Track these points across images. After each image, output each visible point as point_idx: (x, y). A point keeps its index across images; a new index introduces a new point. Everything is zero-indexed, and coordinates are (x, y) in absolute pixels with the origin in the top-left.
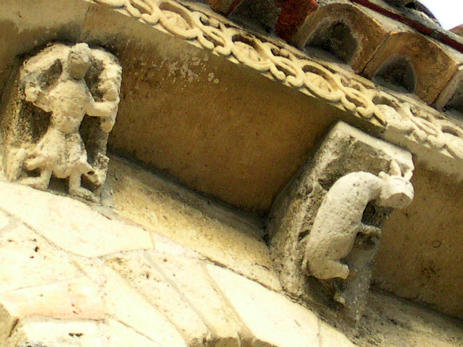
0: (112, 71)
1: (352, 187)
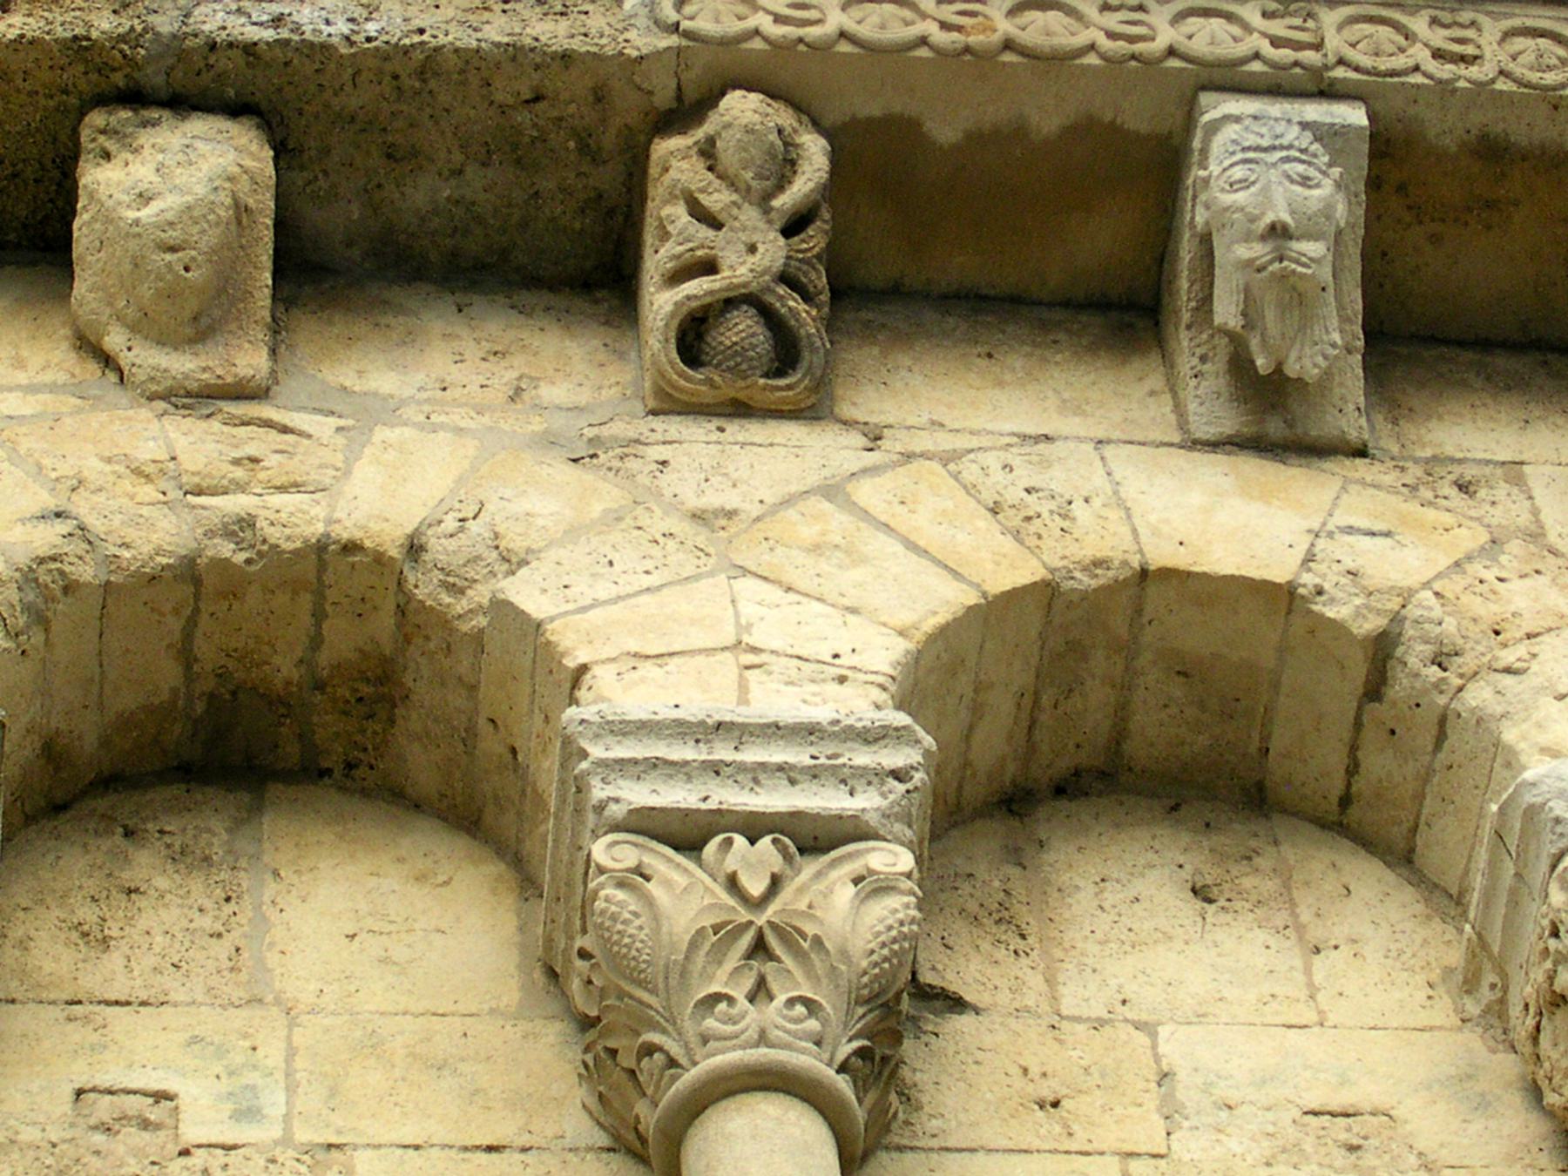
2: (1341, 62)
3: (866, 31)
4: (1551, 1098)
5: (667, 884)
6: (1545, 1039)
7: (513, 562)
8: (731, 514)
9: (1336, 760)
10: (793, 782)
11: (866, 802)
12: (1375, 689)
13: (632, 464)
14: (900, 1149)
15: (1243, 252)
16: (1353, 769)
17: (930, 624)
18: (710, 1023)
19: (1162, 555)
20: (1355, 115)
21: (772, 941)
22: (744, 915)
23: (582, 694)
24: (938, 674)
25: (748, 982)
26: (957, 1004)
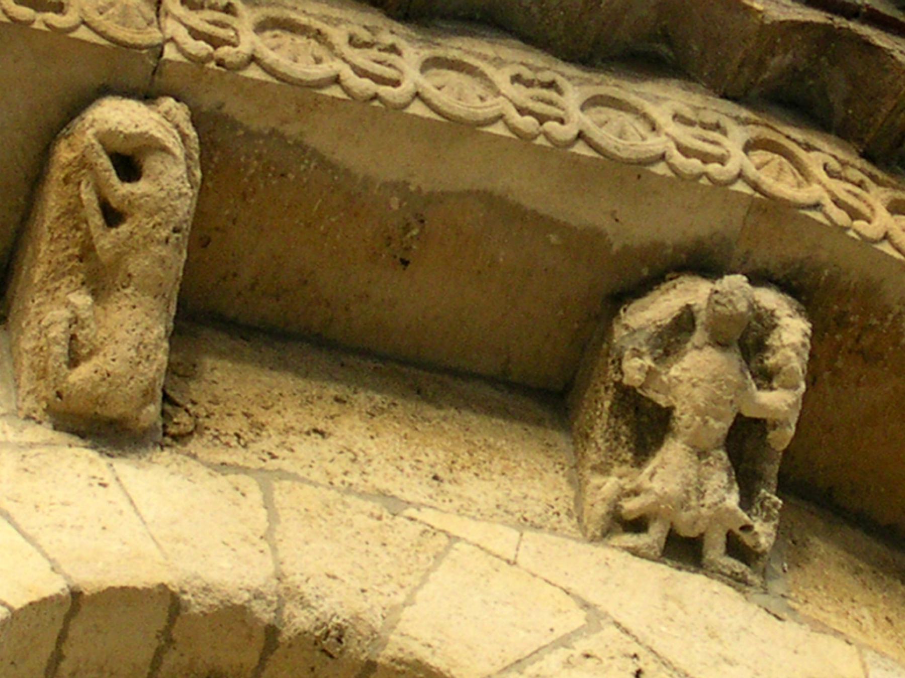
0: (792, 330)
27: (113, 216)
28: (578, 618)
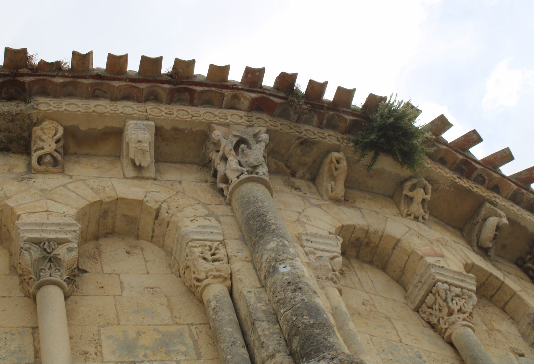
0: (430, 187)
1: (493, 221)
2: (150, 114)
3: (70, 109)
4: (187, 284)
5: (33, 250)
6: (186, 274)
7: (7, 198)
8: (46, 190)
9: (150, 230)
10: (56, 233)
11: (69, 236)
12: (157, 217)
13: (30, 182)
14: (75, 295)
15: (134, 145)
16: (153, 231)
17: (81, 207)
18: (41, 274)
19: (121, 195)
20: (153, 123)
21: (52, 259)
22: (47, 255)
23: (19, 219)
24: (82, 215)
25: (48, 266)
26: (85, 272)
27: (336, 169)
28: (407, 229)
